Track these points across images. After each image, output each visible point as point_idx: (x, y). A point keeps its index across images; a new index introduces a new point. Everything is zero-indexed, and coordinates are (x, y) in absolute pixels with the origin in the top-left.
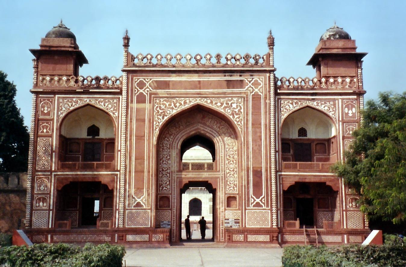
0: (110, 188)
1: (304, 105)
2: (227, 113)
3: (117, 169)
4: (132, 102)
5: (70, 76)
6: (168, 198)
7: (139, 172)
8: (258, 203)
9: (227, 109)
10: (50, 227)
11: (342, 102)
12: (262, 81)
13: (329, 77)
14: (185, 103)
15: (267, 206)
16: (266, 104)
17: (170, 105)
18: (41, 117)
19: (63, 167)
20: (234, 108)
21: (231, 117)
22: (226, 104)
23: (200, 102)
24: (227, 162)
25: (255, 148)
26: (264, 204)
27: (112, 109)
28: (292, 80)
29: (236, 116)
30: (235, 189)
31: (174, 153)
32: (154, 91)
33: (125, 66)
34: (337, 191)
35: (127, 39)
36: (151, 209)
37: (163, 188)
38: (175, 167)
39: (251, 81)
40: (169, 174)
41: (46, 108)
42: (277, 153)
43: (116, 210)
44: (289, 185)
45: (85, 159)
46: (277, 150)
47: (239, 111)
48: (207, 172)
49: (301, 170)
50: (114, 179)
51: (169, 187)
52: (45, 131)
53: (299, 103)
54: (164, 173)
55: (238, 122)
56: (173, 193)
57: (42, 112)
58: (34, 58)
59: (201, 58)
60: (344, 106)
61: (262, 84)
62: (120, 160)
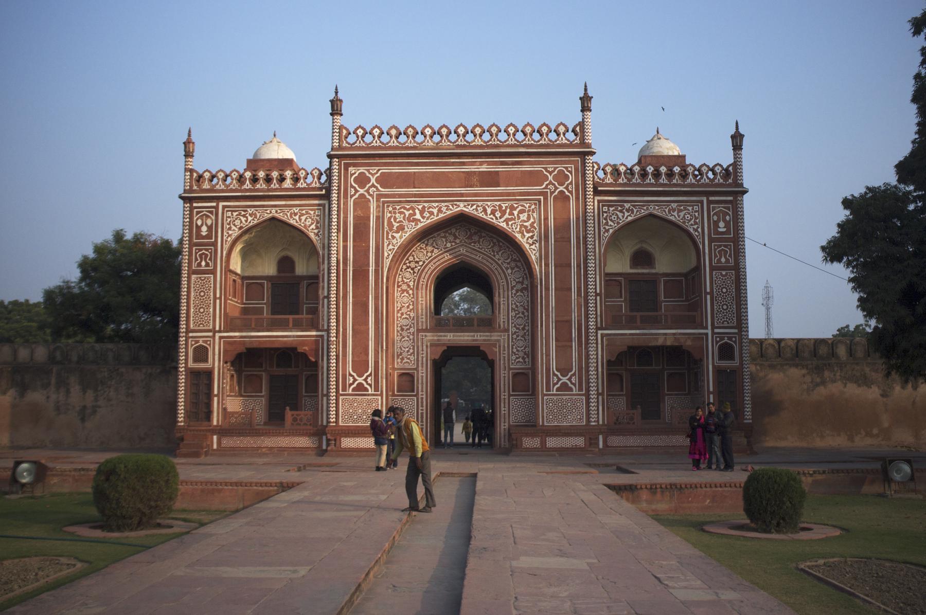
1: (644, 212)
3: (323, 325)
6: (411, 376)
8: (565, 384)
14: (440, 211)
15: (580, 389)
21: (519, 236)
22: (511, 214)
23: (465, 209)
24: (512, 314)
29: (527, 235)
30: (527, 360)
33: (332, 149)
34: (701, 360)
37: (402, 359)
39: (553, 171)
40: (413, 334)
42: (598, 298)
43: (323, 395)
46: (598, 291)
47: (532, 225)
52: (203, 263)
53: (635, 210)
54: (405, 333)
55: (531, 245)
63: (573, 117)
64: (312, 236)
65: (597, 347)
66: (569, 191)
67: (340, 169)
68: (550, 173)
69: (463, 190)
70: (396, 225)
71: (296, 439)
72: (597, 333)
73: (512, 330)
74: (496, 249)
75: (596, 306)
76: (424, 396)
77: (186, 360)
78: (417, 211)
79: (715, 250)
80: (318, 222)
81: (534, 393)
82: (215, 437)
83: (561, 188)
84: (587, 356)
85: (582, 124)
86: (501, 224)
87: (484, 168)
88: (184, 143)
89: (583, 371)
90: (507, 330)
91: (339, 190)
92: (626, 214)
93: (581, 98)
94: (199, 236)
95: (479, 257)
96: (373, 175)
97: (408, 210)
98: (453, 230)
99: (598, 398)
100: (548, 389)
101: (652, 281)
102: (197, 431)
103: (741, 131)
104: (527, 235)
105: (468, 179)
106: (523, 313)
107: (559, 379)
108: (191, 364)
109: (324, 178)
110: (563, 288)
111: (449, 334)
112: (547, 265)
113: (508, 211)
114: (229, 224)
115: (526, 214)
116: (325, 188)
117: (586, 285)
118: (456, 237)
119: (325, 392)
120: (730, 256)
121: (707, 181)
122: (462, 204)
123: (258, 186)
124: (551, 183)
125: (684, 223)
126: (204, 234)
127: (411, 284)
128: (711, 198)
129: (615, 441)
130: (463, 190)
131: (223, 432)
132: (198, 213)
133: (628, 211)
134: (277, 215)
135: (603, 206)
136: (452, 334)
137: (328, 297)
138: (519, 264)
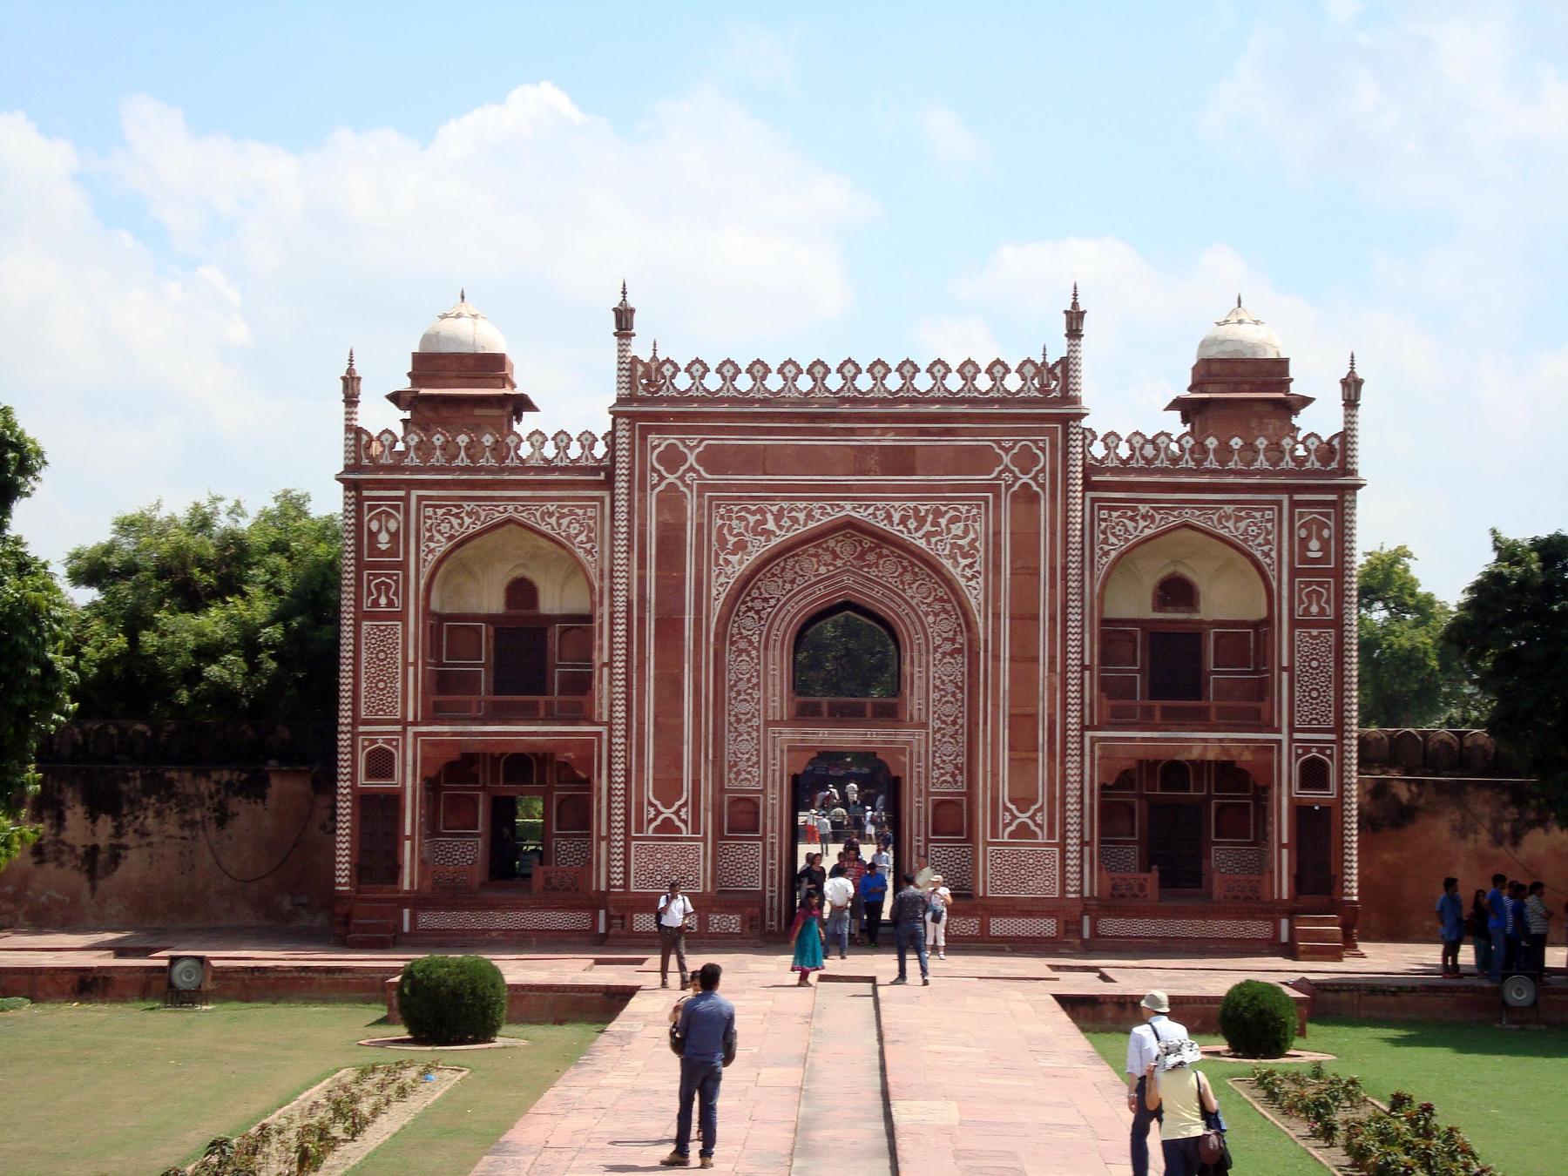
1: (1173, 520)
3: (601, 715)
6: (755, 804)
8: (1023, 825)
9: (933, 540)
12: (1042, 450)
14: (809, 516)
15: (1051, 835)
21: (948, 564)
22: (935, 523)
27: (582, 537)
28: (1138, 442)
29: (964, 562)
30: (959, 778)
33: (621, 401)
34: (1267, 788)
35: (624, 320)
37: (738, 773)
39: (1012, 448)
42: (1087, 673)
43: (600, 838)
45: (499, 688)
47: (972, 544)
52: (383, 601)
53: (1158, 517)
54: (742, 728)
56: (769, 790)
59: (859, 371)
60: (1297, 525)
62: (607, 691)
64: (581, 553)
65: (1082, 761)
66: (1039, 485)
67: (632, 437)
68: (1007, 450)
69: (852, 480)
70: (732, 540)
71: (552, 914)
72: (1082, 736)
73: (934, 724)
74: (908, 577)
75: (1081, 689)
76: (776, 841)
77: (354, 774)
78: (769, 516)
79: (1301, 590)
80: (591, 530)
81: (971, 838)
82: (406, 912)
83: (1025, 479)
84: (1064, 776)
85: (1064, 362)
86: (918, 542)
87: (889, 441)
88: (344, 379)
89: (1057, 802)
90: (924, 725)
91: (631, 475)
92: (1142, 524)
93: (1066, 312)
94: (374, 550)
95: (877, 593)
96: (691, 449)
97: (753, 513)
98: (832, 543)
99: (1082, 851)
100: (995, 834)
101: (1191, 637)
102: (374, 900)
103: (1360, 374)
104: (964, 562)
105: (859, 460)
106: (954, 695)
107: (1014, 817)
108: (362, 781)
110: (1024, 658)
111: (821, 730)
112: (996, 616)
113: (930, 518)
114: (429, 530)
116: (604, 468)
117: (1065, 652)
118: (836, 556)
119: (604, 833)
120: (1328, 602)
121: (1292, 465)
122: (848, 505)
123: (482, 462)
124: (1006, 469)
125: (1245, 540)
126: (383, 547)
127: (755, 639)
128: (1297, 497)
129: (1112, 926)
130: (852, 480)
131: (419, 902)
132: (371, 508)
133: (1144, 518)
134: (517, 516)
135: (1101, 508)
136: (826, 730)
137: (610, 664)
138: (948, 607)
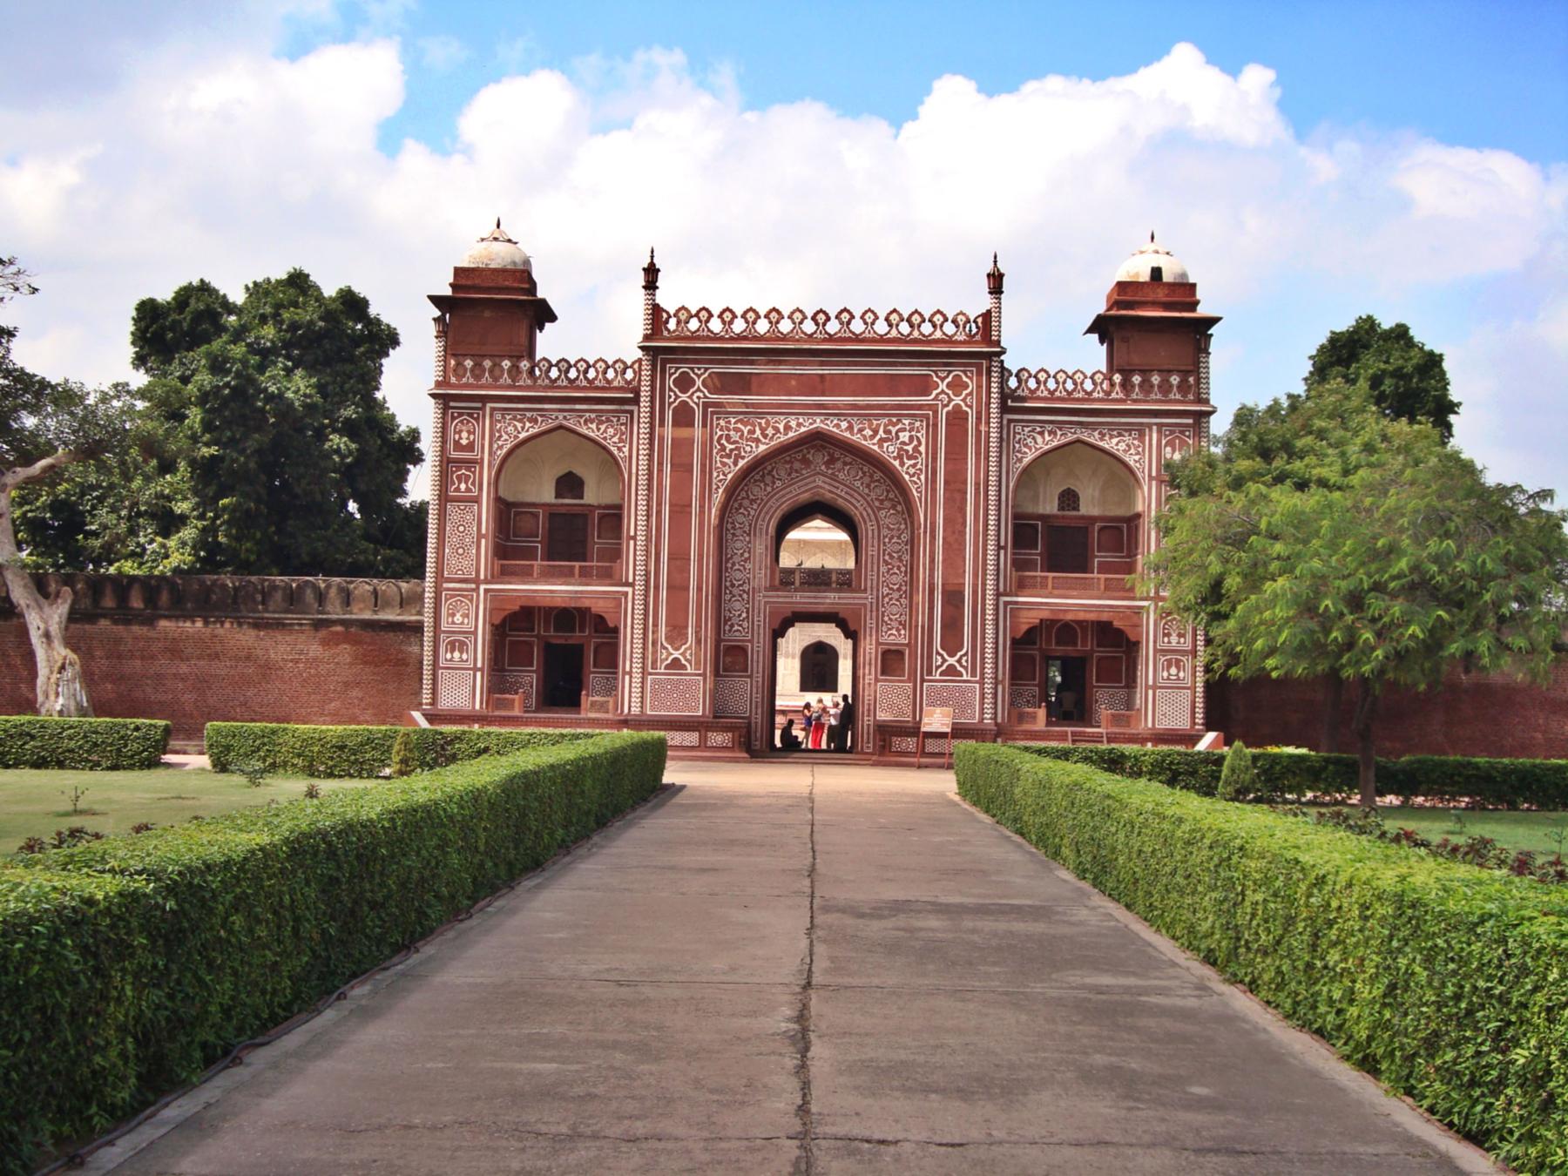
0: (611, 625)
1: (1071, 437)
2: (889, 452)
4: (662, 424)
5: (520, 358)
6: (743, 650)
7: (678, 588)
10: (477, 707)
11: (1159, 432)
13: (1132, 372)
14: (788, 428)
15: (974, 675)
16: (978, 432)
17: (752, 432)
18: (455, 455)
19: (504, 574)
20: (903, 443)
21: (896, 463)
22: (887, 432)
25: (951, 539)
26: (966, 668)
27: (615, 439)
28: (1042, 376)
29: (909, 463)
31: (761, 546)
32: (715, 397)
33: (647, 338)
34: (1137, 644)
35: (651, 273)
36: (704, 675)
38: (759, 575)
41: (464, 435)
43: (624, 673)
44: (1024, 628)
47: (916, 449)
48: (835, 591)
49: (1056, 592)
50: (618, 600)
51: (745, 624)
52: (463, 486)
57: (457, 443)
58: (437, 313)
59: (828, 319)
61: (972, 386)
63: (981, 302)
72: (997, 600)
85: (989, 312)
109: (629, 375)
115: (907, 434)
134: (565, 423)
